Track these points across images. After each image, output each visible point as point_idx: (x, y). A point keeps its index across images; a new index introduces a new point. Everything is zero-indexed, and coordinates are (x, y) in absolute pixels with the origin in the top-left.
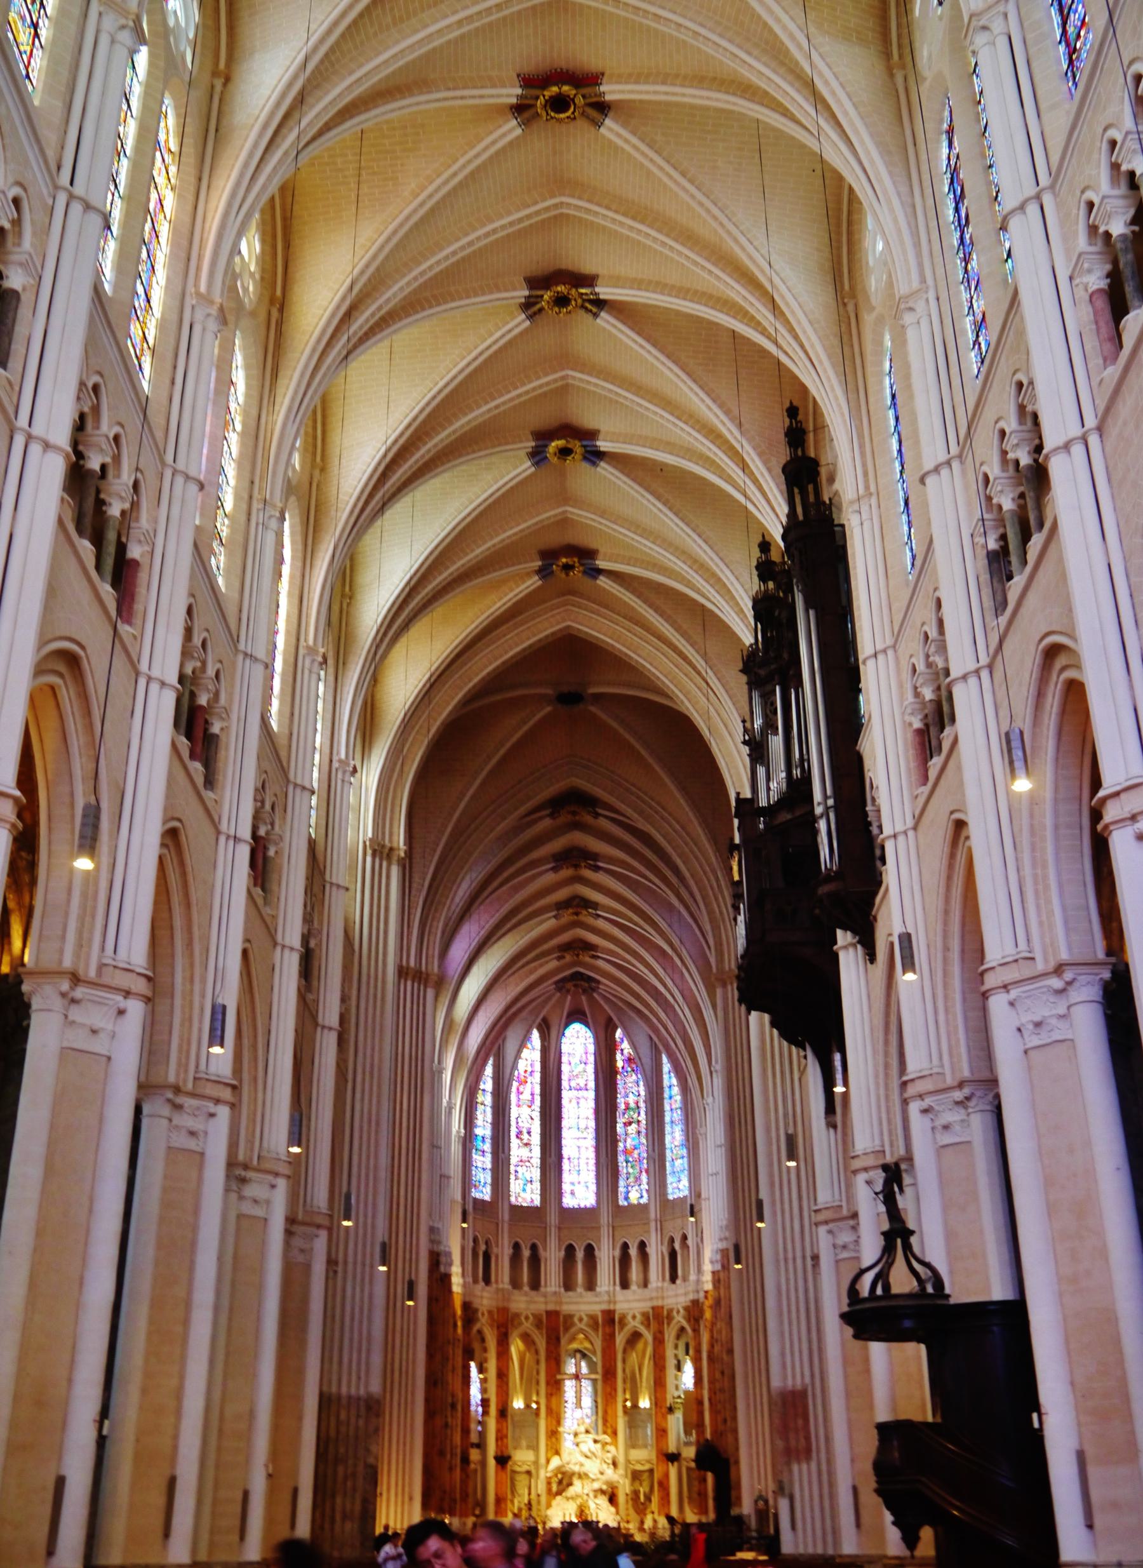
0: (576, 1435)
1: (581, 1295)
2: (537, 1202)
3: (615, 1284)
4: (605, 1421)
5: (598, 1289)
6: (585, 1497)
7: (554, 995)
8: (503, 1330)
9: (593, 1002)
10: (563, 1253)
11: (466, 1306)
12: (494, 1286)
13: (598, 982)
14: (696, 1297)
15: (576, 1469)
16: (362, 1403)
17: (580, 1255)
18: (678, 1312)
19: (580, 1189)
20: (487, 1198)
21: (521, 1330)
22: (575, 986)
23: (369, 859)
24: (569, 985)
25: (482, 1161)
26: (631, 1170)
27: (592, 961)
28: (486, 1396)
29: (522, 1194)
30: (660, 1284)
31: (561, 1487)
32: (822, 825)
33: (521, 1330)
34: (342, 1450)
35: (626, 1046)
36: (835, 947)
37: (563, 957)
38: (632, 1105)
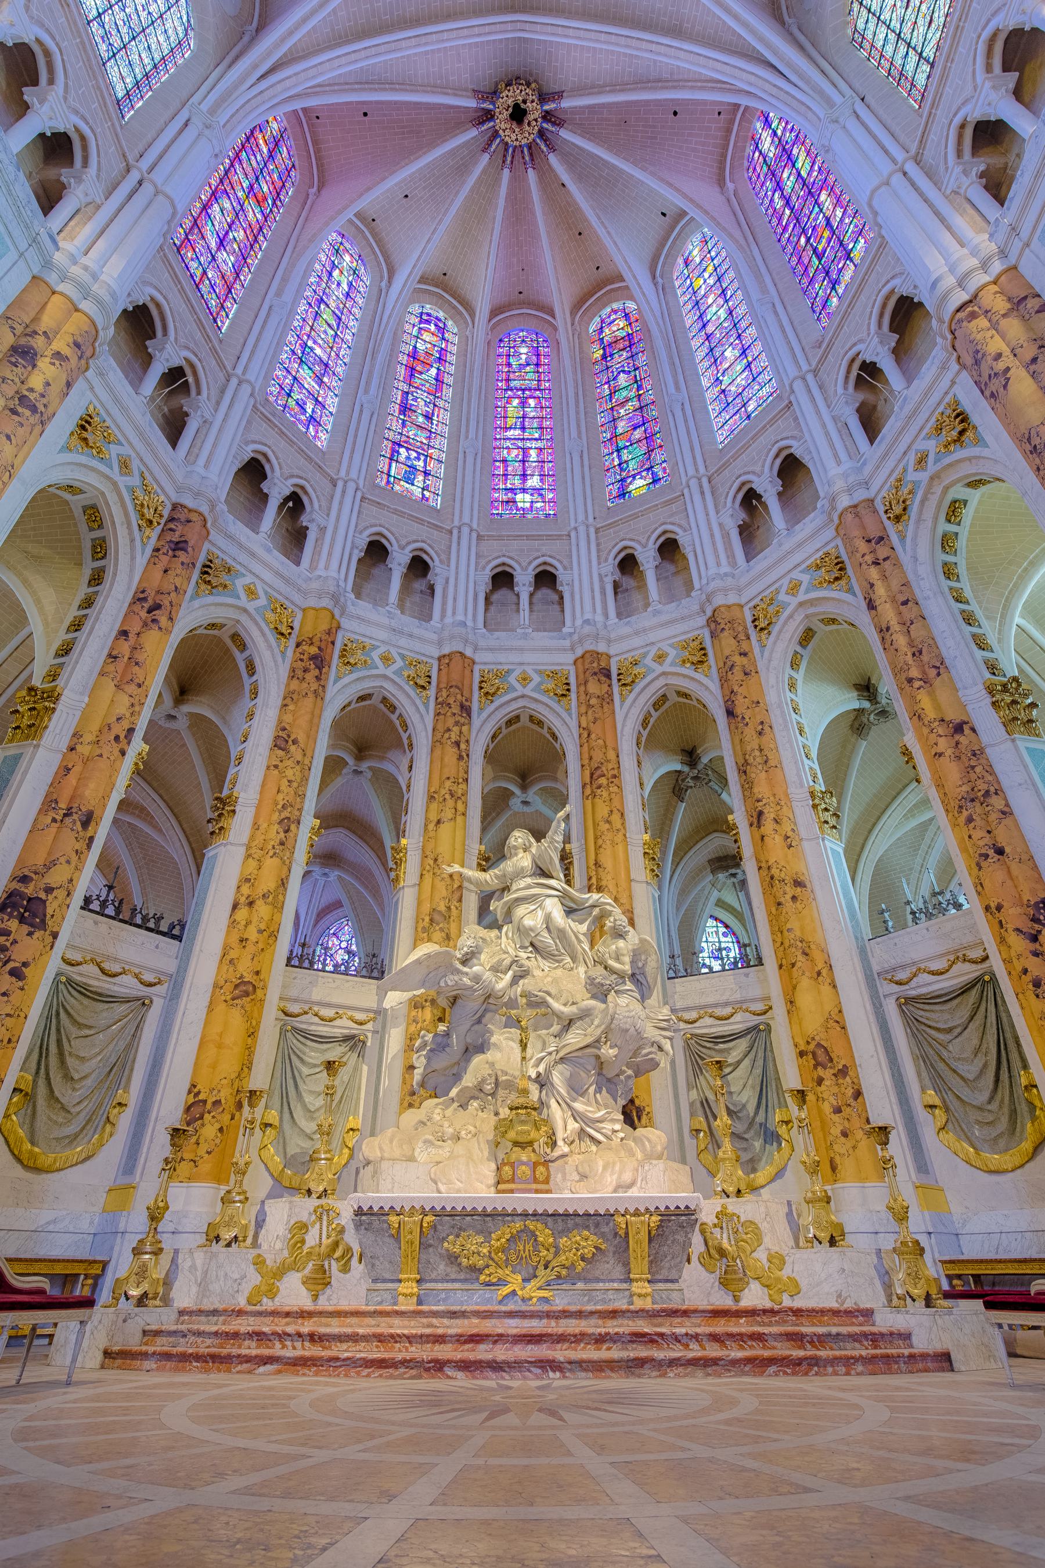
1: (525, 636)
5: (565, 630)
8: (313, 650)
14: (861, 495)
31: (442, 1062)
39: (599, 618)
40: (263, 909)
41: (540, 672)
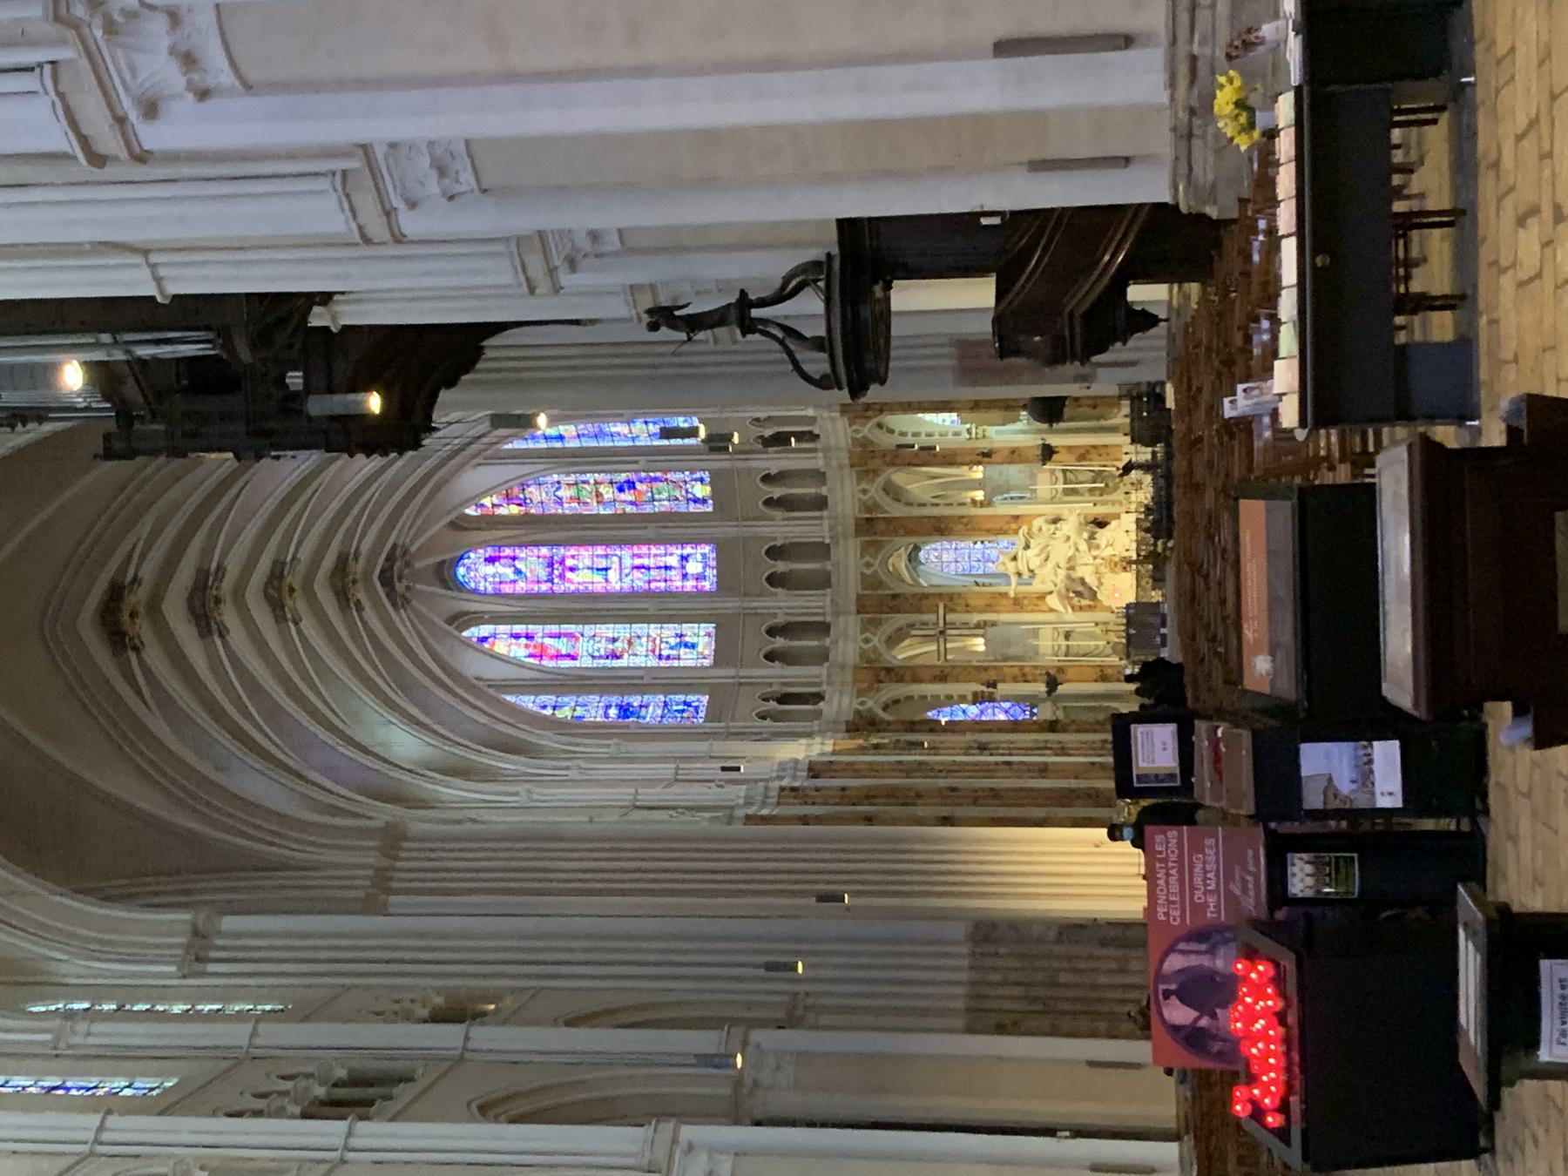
0: (1019, 574)
1: (836, 565)
2: (711, 627)
3: (821, 518)
4: (1002, 532)
6: (1099, 561)
7: (414, 610)
9: (426, 550)
10: (779, 590)
11: (853, 728)
12: (825, 687)
13: (395, 546)
15: (1062, 573)
16: (978, 950)
17: (781, 566)
18: (857, 431)
19: (695, 566)
20: (705, 699)
21: (882, 649)
22: (400, 580)
23: (212, 968)
24: (400, 587)
25: (653, 709)
26: (664, 495)
27: (362, 560)
28: (970, 698)
29: (700, 649)
30: (820, 455)
32: (144, 352)
33: (882, 649)
34: (1040, 977)
35: (487, 501)
36: (334, 330)
37: (358, 604)
38: (572, 492)
39: (826, 523)
40: (1026, 670)
41: (862, 557)
